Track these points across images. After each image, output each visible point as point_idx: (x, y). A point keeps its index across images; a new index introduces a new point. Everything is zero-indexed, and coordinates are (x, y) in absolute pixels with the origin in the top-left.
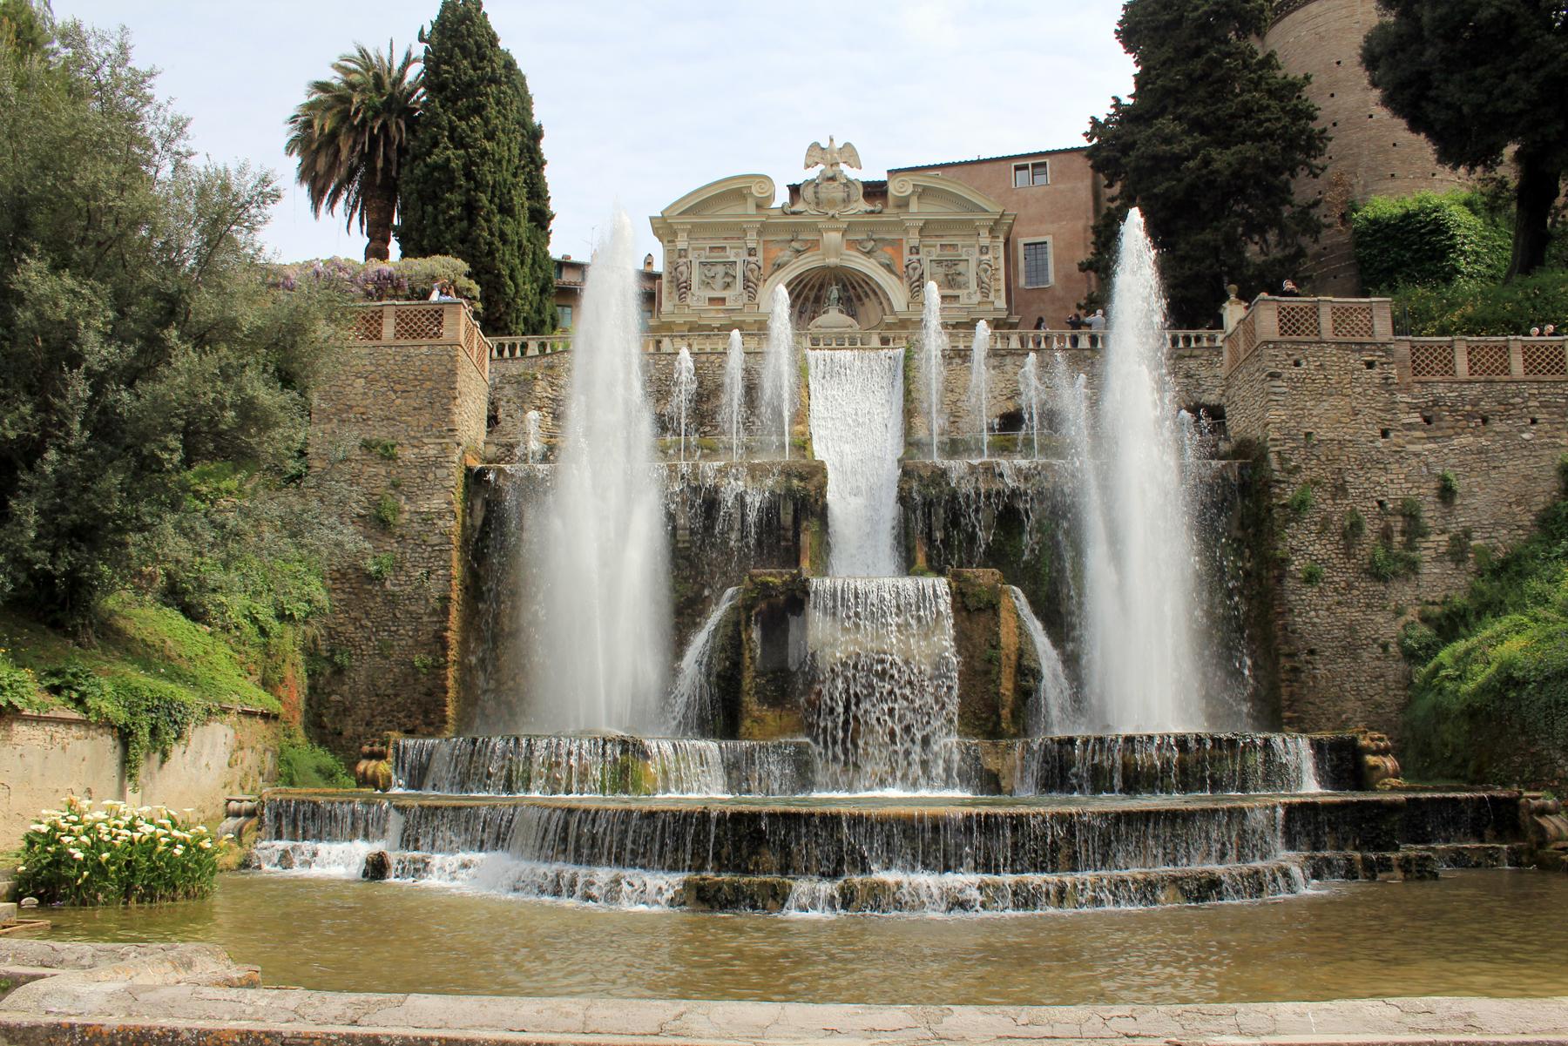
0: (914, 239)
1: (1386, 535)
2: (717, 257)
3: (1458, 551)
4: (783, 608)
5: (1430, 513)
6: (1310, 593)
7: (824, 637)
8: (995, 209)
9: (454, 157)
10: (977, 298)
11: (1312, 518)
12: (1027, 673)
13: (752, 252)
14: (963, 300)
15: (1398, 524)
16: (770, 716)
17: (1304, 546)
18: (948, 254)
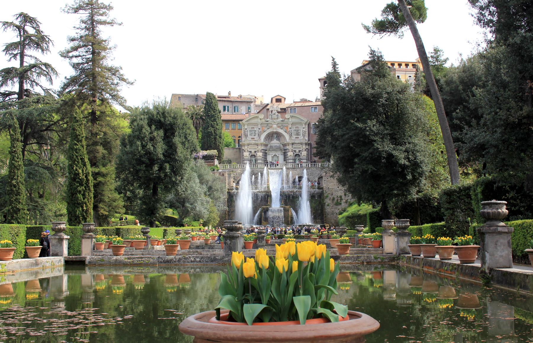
0: (290, 126)
1: (338, 200)
2: (253, 129)
3: (346, 202)
4: (266, 211)
5: (343, 197)
6: (328, 207)
7: (270, 214)
8: (306, 120)
9: (212, 130)
10: (302, 138)
11: (328, 198)
12: (292, 218)
13: (259, 129)
14: (300, 138)
15: (339, 198)
16: (265, 223)
17: (327, 201)
18: (297, 129)
